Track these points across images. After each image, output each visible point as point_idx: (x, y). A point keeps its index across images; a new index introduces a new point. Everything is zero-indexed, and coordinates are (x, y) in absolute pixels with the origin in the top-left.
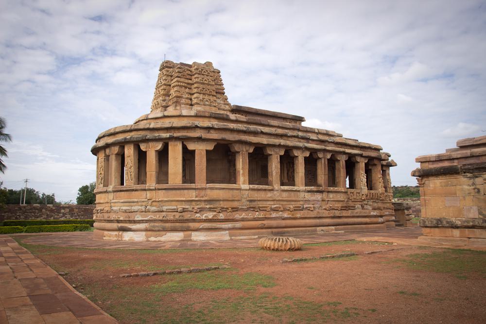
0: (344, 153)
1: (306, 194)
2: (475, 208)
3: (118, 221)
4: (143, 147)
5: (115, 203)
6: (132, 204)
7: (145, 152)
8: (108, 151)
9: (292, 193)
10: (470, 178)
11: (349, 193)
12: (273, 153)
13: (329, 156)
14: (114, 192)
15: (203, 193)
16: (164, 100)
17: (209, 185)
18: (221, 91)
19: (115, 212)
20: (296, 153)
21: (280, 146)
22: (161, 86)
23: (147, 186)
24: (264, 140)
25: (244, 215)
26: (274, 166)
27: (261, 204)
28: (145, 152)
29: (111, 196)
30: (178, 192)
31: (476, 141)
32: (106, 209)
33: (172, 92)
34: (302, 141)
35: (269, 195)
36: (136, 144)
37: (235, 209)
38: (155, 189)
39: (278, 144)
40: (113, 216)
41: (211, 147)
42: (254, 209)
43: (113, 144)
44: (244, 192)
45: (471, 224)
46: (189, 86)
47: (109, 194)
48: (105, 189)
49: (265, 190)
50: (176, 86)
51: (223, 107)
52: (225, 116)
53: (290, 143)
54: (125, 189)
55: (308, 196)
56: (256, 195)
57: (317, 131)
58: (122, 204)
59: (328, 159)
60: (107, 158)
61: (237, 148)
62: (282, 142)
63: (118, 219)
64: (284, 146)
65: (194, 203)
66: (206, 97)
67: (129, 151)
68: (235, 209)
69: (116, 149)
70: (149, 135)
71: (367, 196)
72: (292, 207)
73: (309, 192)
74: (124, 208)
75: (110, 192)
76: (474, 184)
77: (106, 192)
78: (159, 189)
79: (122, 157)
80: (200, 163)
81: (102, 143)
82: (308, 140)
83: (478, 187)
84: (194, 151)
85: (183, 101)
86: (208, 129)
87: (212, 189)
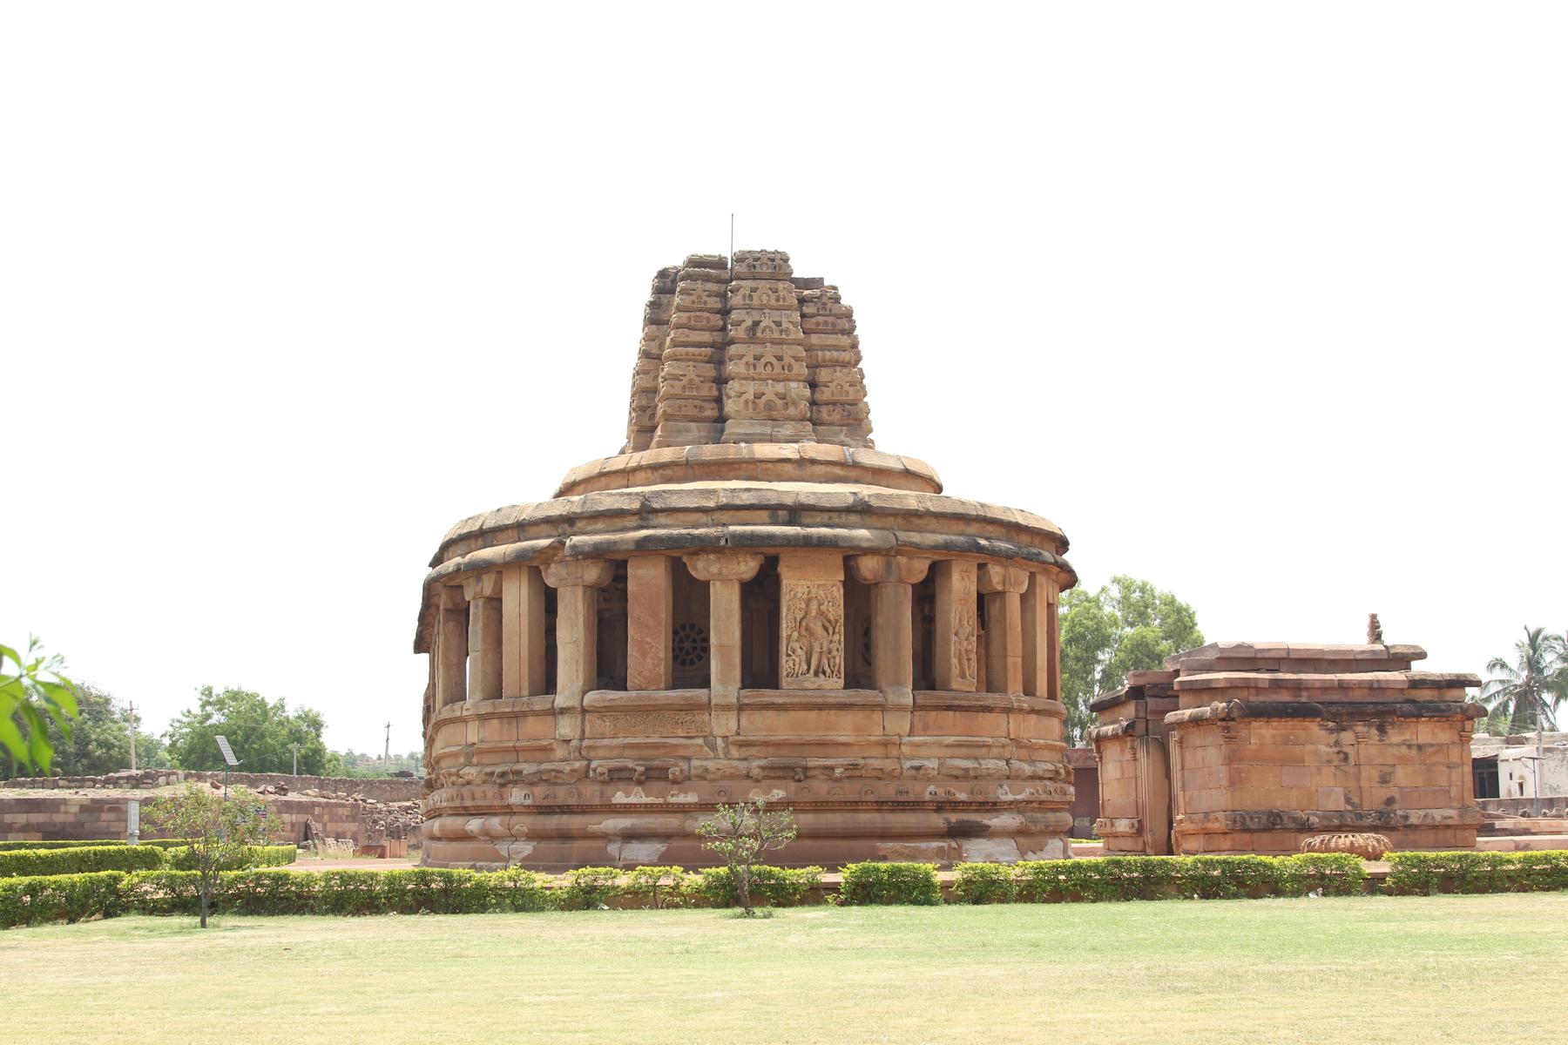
2: (1339, 791)
3: (940, 807)
5: (917, 745)
6: (977, 752)
10: (1332, 731)
22: (781, 342)
29: (899, 724)
31: (1262, 651)
32: (889, 765)
33: (823, 375)
40: (929, 791)
45: (1336, 822)
47: (888, 716)
54: (964, 703)
58: (948, 752)
63: (951, 798)
67: (961, 586)
75: (900, 708)
76: (1337, 743)
83: (1346, 749)
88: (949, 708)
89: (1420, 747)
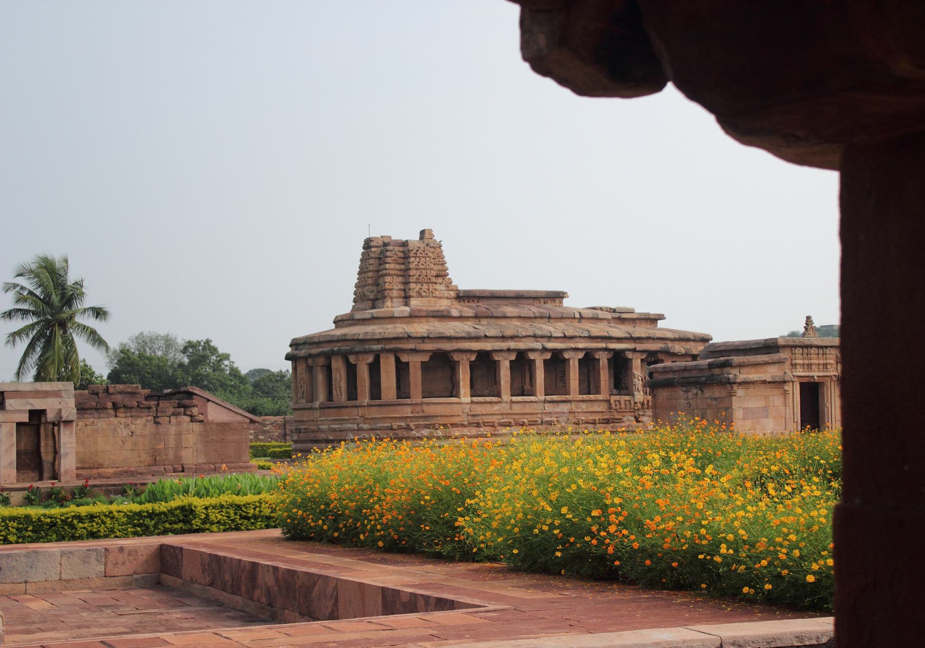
0: (606, 349)
1: (546, 405)
4: (352, 359)
7: (355, 365)
8: (310, 361)
9: (527, 405)
11: (612, 401)
12: (500, 359)
13: (581, 355)
14: (321, 408)
15: (418, 408)
16: (372, 292)
17: (426, 400)
18: (443, 273)
19: (322, 431)
20: (532, 356)
21: (509, 350)
23: (358, 402)
24: (488, 346)
25: (466, 431)
26: (502, 373)
27: (486, 419)
28: (355, 365)
29: (317, 413)
30: (392, 408)
32: (312, 427)
34: (541, 340)
35: (496, 408)
36: (345, 356)
37: (454, 425)
38: (369, 406)
39: (505, 348)
41: (426, 358)
42: (478, 425)
43: (318, 355)
44: (464, 406)
46: (402, 273)
48: (309, 405)
49: (491, 403)
50: (386, 275)
51: (446, 294)
52: (445, 313)
53: (521, 345)
55: (549, 408)
56: (479, 409)
57: (577, 316)
59: (579, 360)
60: (310, 369)
61: (456, 357)
62: (512, 345)
64: (514, 350)
65: (409, 420)
66: (425, 287)
67: (338, 365)
68: (454, 425)
69: (321, 361)
70: (358, 348)
71: (643, 404)
72: (526, 421)
73: (549, 402)
74: (336, 426)
75: (316, 409)
76: (687, 399)
77: (311, 409)
78: (372, 406)
79: (328, 369)
80: (416, 376)
81: (303, 352)
82: (550, 338)
84: (407, 363)
85: (395, 293)
86: (423, 339)
87: (428, 404)
88: (329, 408)
89: (715, 399)
